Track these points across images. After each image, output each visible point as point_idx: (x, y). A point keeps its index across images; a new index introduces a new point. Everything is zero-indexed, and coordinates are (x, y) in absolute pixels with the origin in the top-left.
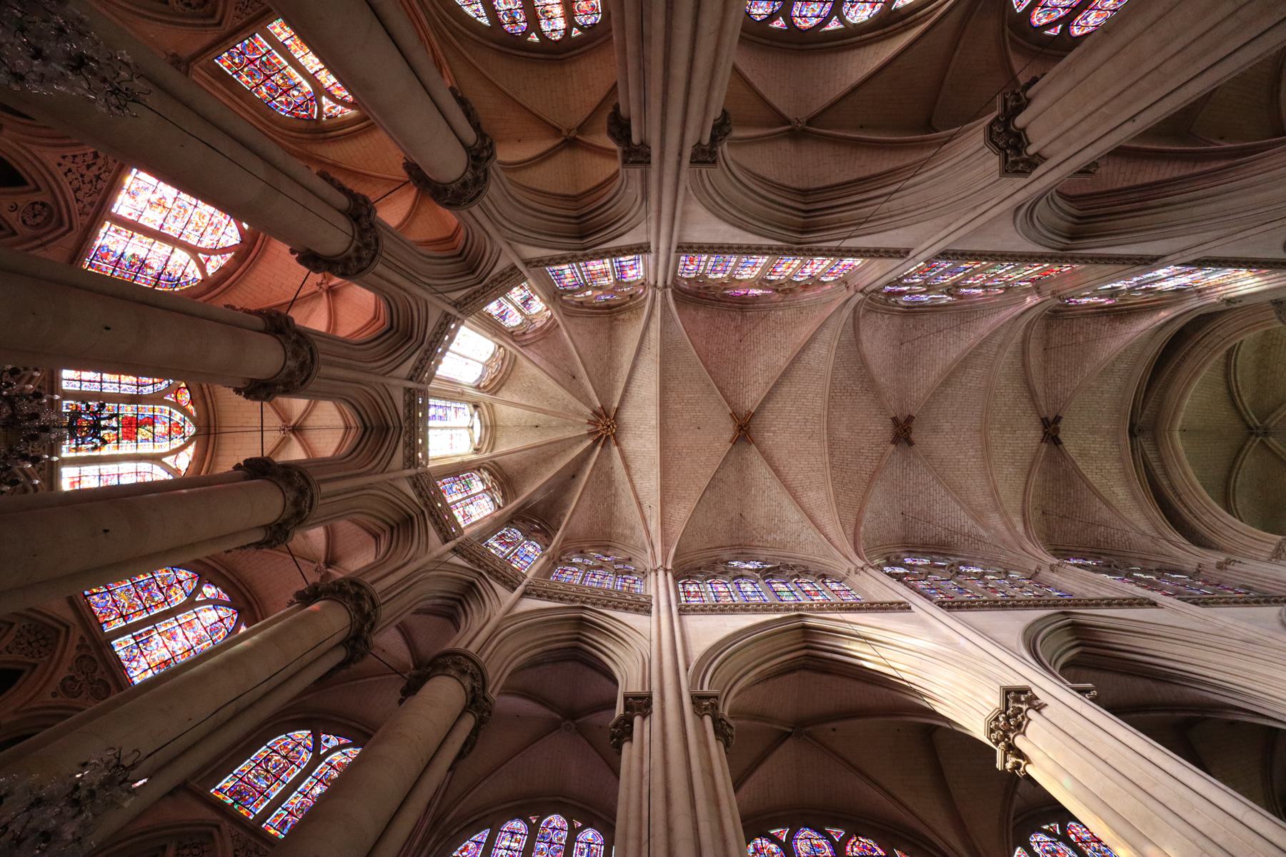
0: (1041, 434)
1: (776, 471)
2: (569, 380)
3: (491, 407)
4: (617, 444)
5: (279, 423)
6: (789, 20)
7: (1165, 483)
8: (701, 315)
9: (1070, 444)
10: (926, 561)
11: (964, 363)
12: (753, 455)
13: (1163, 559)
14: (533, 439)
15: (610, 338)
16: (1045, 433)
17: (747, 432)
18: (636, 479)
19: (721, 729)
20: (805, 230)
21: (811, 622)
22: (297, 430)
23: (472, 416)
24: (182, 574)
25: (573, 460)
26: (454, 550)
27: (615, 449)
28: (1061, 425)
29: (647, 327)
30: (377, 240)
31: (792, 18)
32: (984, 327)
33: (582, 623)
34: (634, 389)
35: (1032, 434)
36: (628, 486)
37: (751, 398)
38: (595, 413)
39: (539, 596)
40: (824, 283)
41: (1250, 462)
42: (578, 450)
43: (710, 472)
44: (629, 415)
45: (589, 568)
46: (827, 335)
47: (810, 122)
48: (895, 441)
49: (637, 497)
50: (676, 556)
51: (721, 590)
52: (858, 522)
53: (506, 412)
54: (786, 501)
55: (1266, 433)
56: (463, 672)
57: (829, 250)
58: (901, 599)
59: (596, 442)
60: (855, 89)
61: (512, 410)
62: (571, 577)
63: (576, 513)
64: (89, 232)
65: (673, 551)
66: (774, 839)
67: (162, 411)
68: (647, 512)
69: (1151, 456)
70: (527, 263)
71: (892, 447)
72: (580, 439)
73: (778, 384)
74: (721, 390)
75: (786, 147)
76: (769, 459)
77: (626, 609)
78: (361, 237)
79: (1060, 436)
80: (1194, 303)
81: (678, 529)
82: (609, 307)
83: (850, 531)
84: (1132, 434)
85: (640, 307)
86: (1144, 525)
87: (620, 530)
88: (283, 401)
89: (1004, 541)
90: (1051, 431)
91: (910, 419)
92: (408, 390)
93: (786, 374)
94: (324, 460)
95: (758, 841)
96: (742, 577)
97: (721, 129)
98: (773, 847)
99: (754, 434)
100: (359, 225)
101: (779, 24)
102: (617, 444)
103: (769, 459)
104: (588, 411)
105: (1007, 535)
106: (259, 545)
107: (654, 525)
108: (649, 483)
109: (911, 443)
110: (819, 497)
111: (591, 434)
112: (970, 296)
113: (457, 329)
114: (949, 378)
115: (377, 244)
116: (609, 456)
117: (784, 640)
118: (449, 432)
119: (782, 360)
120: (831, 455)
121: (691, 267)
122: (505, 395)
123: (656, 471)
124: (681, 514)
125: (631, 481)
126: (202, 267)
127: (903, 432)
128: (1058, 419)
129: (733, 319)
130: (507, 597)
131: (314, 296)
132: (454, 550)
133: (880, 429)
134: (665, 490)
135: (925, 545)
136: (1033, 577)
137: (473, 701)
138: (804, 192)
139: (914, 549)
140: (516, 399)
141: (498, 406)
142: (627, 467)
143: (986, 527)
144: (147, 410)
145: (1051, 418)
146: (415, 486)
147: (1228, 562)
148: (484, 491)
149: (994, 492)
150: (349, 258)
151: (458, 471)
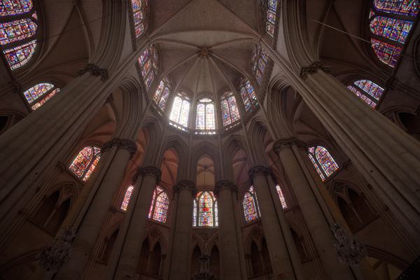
4: (211, 47)
5: (203, 173)
6: (31, 12)
19: (312, 70)
22: (206, 167)
23: (201, 103)
24: (246, 196)
26: (245, 125)
27: (213, 48)
29: (165, 40)
31: (31, 10)
33: (273, 89)
38: (199, 56)
39: (263, 99)
42: (213, 62)
44: (200, 42)
45: (257, 67)
49: (232, 41)
50: (257, 30)
51: (271, 16)
53: (199, 90)
59: (210, 55)
61: (199, 87)
63: (238, 64)
64: (157, 223)
65: (254, 31)
66: (372, 18)
67: (201, 200)
68: (238, 37)
70: (148, 104)
72: (210, 62)
77: (272, 70)
78: (149, 173)
81: (246, 27)
85: (158, 44)
95: (371, 25)
97: (96, 71)
98: (375, 20)
101: (34, 15)
102: (211, 47)
106: (237, 192)
107: (243, 36)
108: (228, 36)
111: (207, 58)
113: (172, 122)
121: (140, 29)
123: (223, 33)
124: (240, 24)
126: (161, 193)
132: (245, 125)
134: (231, 30)
137: (289, 143)
141: (198, 92)
142: (220, 43)
144: (201, 205)
146: (224, 136)
148: (227, 100)
151: (219, 113)
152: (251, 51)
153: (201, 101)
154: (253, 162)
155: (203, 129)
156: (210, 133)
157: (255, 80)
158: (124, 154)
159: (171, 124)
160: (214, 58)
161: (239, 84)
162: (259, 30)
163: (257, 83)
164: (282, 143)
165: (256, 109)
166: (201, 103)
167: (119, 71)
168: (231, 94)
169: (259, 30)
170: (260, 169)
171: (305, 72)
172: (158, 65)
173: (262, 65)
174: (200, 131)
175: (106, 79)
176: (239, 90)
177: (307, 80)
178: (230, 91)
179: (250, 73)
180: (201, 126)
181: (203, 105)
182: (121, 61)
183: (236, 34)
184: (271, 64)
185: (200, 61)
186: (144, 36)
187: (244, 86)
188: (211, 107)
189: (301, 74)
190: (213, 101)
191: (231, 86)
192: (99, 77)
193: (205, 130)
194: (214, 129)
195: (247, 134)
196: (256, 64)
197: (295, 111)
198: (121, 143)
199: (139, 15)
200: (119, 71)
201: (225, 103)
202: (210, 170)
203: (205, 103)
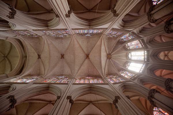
0: (41, 56)
1: (83, 50)
2: (115, 63)
3: (127, 59)
7: (22, 49)
8: (95, 74)
9: (36, 54)
10: (59, 36)
11: (54, 67)
12: (86, 52)
13: (24, 37)
14: (120, 54)
15: (109, 70)
16: (40, 56)
17: (87, 56)
18: (104, 48)
19: (115, 12)
20: (91, 87)
21: (89, 27)
22: (166, 55)
23: (131, 58)
25: (114, 51)
26: (141, 38)
27: (108, 53)
28: (38, 57)
29: (104, 72)
30: (165, 84)
32: (51, 73)
33: (124, 27)
34: (105, 62)
35: (41, 56)
36: (106, 47)
37: (87, 61)
40: (78, 79)
41: (7, 52)
42: (113, 53)
43: (93, 50)
44: (105, 58)
45: (114, 35)
46: (76, 71)
47: (89, 104)
48: (64, 55)
49: (105, 46)
50: (101, 36)
51: (95, 31)
52: (70, 42)
53: (125, 58)
54: (81, 45)
55: (4, 57)
56: (153, 20)
57: (85, 84)
58: (72, 30)
59: (111, 54)
60: (83, 109)
62: (119, 33)
63: (114, 42)
69: (23, 53)
70: (131, 81)
71: (64, 54)
72: (113, 54)
73: (83, 63)
74: (91, 63)
75: (92, 100)
76: (84, 52)
78: (169, 84)
79: (38, 56)
80: (20, 77)
82: (109, 75)
83: (72, 41)
84: (26, 56)
85: (106, 75)
86: (26, 42)
87: (107, 40)
88: (167, 59)
89: (48, 39)
90: (39, 57)
91: (61, 58)
92: (149, 62)
93: (81, 65)
94: (163, 51)
96: (91, 33)
97: (116, 101)
99: (86, 56)
100: (169, 86)
103: (84, 52)
104: (112, 59)
105: (48, 40)
108: (103, 47)
109: (61, 54)
110: (77, 46)
111: (111, 55)
112: (54, 78)
114: (56, 65)
115: (165, 84)
116: (108, 52)
117: (94, 24)
118: (136, 55)
119: (82, 67)
120: (74, 53)
121: (100, 81)
122: (125, 61)
124: (98, 43)
125: (105, 48)
127: (62, 56)
128: (38, 59)
129: (89, 73)
130: (135, 31)
131: (164, 76)
132: (141, 38)
133: (66, 57)
134: (101, 47)
135: (59, 39)
136: (46, 34)
137: (150, 15)
138: (91, 93)
139: (62, 38)
140: (123, 60)
142: (106, 50)
143: (51, 41)
145: (39, 59)
146: (147, 47)
147: (15, 36)
149: (49, 47)
150: (171, 81)
151: (135, 49)
152: (109, 38)
153: (130, 58)
154: (162, 32)
155: (143, 57)
156: (146, 54)
157: (120, 35)
158: (157, 95)
159: (141, 72)
160: (112, 53)
161: (122, 42)
162: (100, 35)
163: (122, 34)
164: (151, 19)
165: (133, 33)
166: (131, 58)
167: (116, 91)
168: (127, 45)
169: (100, 35)
170: (167, 28)
171: (116, 14)
172: (114, 75)
173: (114, 33)
174: (145, 59)
175: (119, 98)
176: (125, 42)
177: (119, 13)
178: (125, 45)
179: (117, 37)
180: (142, 58)
181: (132, 57)
182: (112, 90)
183: (102, 44)
184: (113, 29)
185: (113, 58)
186: (103, 80)
187: (123, 39)
188: (133, 53)
189: (116, 16)
190: (130, 53)
191: (123, 45)
192: (118, 100)
193: (144, 56)
194: (143, 52)
195: (146, 36)
196: (113, 35)
197: (133, 15)
198: (151, 96)
199: (95, 81)
200: (116, 91)
201: (131, 47)
202: (168, 53)
203: (131, 56)
